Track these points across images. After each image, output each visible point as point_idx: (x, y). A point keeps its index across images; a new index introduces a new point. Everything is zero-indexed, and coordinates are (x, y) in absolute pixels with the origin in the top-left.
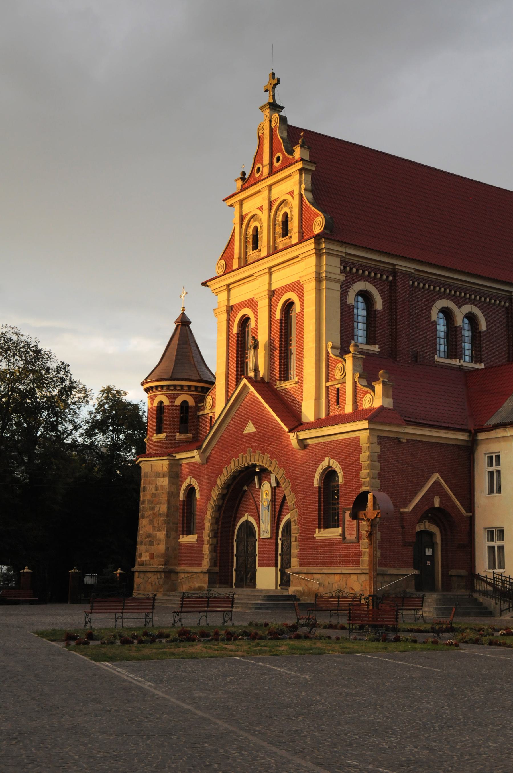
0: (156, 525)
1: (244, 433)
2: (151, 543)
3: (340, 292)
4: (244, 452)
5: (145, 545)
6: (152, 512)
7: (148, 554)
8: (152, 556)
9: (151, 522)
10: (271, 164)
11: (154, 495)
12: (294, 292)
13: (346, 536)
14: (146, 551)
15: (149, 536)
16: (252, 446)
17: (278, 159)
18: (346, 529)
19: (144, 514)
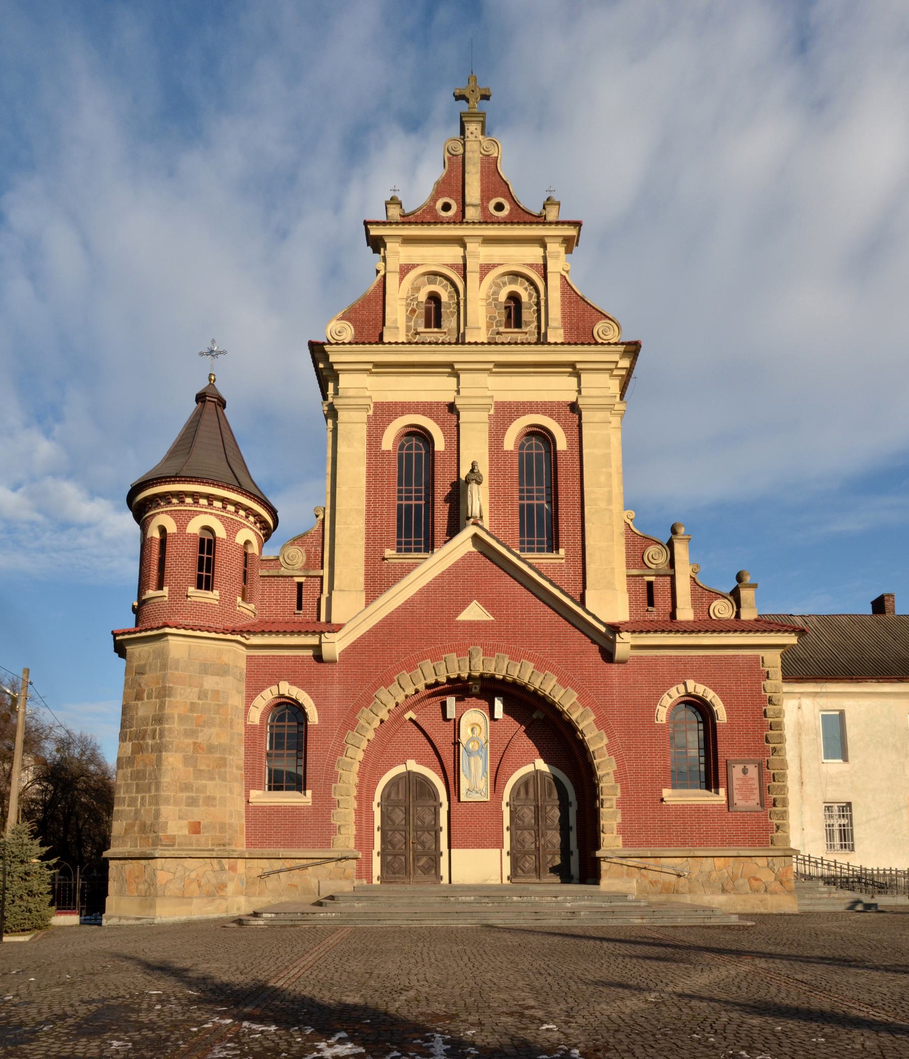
0: (204, 767)
1: (459, 618)
2: (192, 802)
3: (487, 426)
4: (463, 651)
5: (176, 803)
6: (191, 741)
7: (184, 823)
8: (196, 828)
9: (189, 761)
10: (484, 209)
11: (193, 707)
12: (551, 416)
13: (735, 801)
14: (180, 818)
15: (187, 787)
16: (482, 645)
17: (499, 207)
18: (735, 792)
19: (171, 743)
